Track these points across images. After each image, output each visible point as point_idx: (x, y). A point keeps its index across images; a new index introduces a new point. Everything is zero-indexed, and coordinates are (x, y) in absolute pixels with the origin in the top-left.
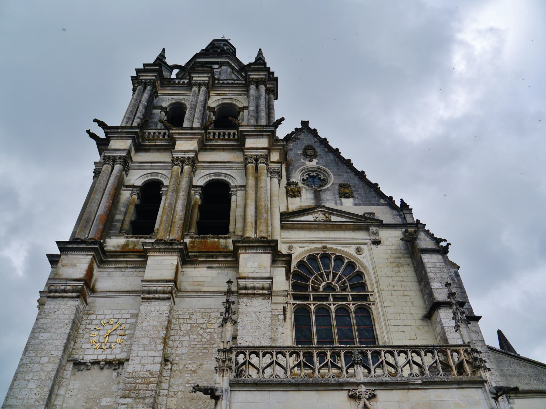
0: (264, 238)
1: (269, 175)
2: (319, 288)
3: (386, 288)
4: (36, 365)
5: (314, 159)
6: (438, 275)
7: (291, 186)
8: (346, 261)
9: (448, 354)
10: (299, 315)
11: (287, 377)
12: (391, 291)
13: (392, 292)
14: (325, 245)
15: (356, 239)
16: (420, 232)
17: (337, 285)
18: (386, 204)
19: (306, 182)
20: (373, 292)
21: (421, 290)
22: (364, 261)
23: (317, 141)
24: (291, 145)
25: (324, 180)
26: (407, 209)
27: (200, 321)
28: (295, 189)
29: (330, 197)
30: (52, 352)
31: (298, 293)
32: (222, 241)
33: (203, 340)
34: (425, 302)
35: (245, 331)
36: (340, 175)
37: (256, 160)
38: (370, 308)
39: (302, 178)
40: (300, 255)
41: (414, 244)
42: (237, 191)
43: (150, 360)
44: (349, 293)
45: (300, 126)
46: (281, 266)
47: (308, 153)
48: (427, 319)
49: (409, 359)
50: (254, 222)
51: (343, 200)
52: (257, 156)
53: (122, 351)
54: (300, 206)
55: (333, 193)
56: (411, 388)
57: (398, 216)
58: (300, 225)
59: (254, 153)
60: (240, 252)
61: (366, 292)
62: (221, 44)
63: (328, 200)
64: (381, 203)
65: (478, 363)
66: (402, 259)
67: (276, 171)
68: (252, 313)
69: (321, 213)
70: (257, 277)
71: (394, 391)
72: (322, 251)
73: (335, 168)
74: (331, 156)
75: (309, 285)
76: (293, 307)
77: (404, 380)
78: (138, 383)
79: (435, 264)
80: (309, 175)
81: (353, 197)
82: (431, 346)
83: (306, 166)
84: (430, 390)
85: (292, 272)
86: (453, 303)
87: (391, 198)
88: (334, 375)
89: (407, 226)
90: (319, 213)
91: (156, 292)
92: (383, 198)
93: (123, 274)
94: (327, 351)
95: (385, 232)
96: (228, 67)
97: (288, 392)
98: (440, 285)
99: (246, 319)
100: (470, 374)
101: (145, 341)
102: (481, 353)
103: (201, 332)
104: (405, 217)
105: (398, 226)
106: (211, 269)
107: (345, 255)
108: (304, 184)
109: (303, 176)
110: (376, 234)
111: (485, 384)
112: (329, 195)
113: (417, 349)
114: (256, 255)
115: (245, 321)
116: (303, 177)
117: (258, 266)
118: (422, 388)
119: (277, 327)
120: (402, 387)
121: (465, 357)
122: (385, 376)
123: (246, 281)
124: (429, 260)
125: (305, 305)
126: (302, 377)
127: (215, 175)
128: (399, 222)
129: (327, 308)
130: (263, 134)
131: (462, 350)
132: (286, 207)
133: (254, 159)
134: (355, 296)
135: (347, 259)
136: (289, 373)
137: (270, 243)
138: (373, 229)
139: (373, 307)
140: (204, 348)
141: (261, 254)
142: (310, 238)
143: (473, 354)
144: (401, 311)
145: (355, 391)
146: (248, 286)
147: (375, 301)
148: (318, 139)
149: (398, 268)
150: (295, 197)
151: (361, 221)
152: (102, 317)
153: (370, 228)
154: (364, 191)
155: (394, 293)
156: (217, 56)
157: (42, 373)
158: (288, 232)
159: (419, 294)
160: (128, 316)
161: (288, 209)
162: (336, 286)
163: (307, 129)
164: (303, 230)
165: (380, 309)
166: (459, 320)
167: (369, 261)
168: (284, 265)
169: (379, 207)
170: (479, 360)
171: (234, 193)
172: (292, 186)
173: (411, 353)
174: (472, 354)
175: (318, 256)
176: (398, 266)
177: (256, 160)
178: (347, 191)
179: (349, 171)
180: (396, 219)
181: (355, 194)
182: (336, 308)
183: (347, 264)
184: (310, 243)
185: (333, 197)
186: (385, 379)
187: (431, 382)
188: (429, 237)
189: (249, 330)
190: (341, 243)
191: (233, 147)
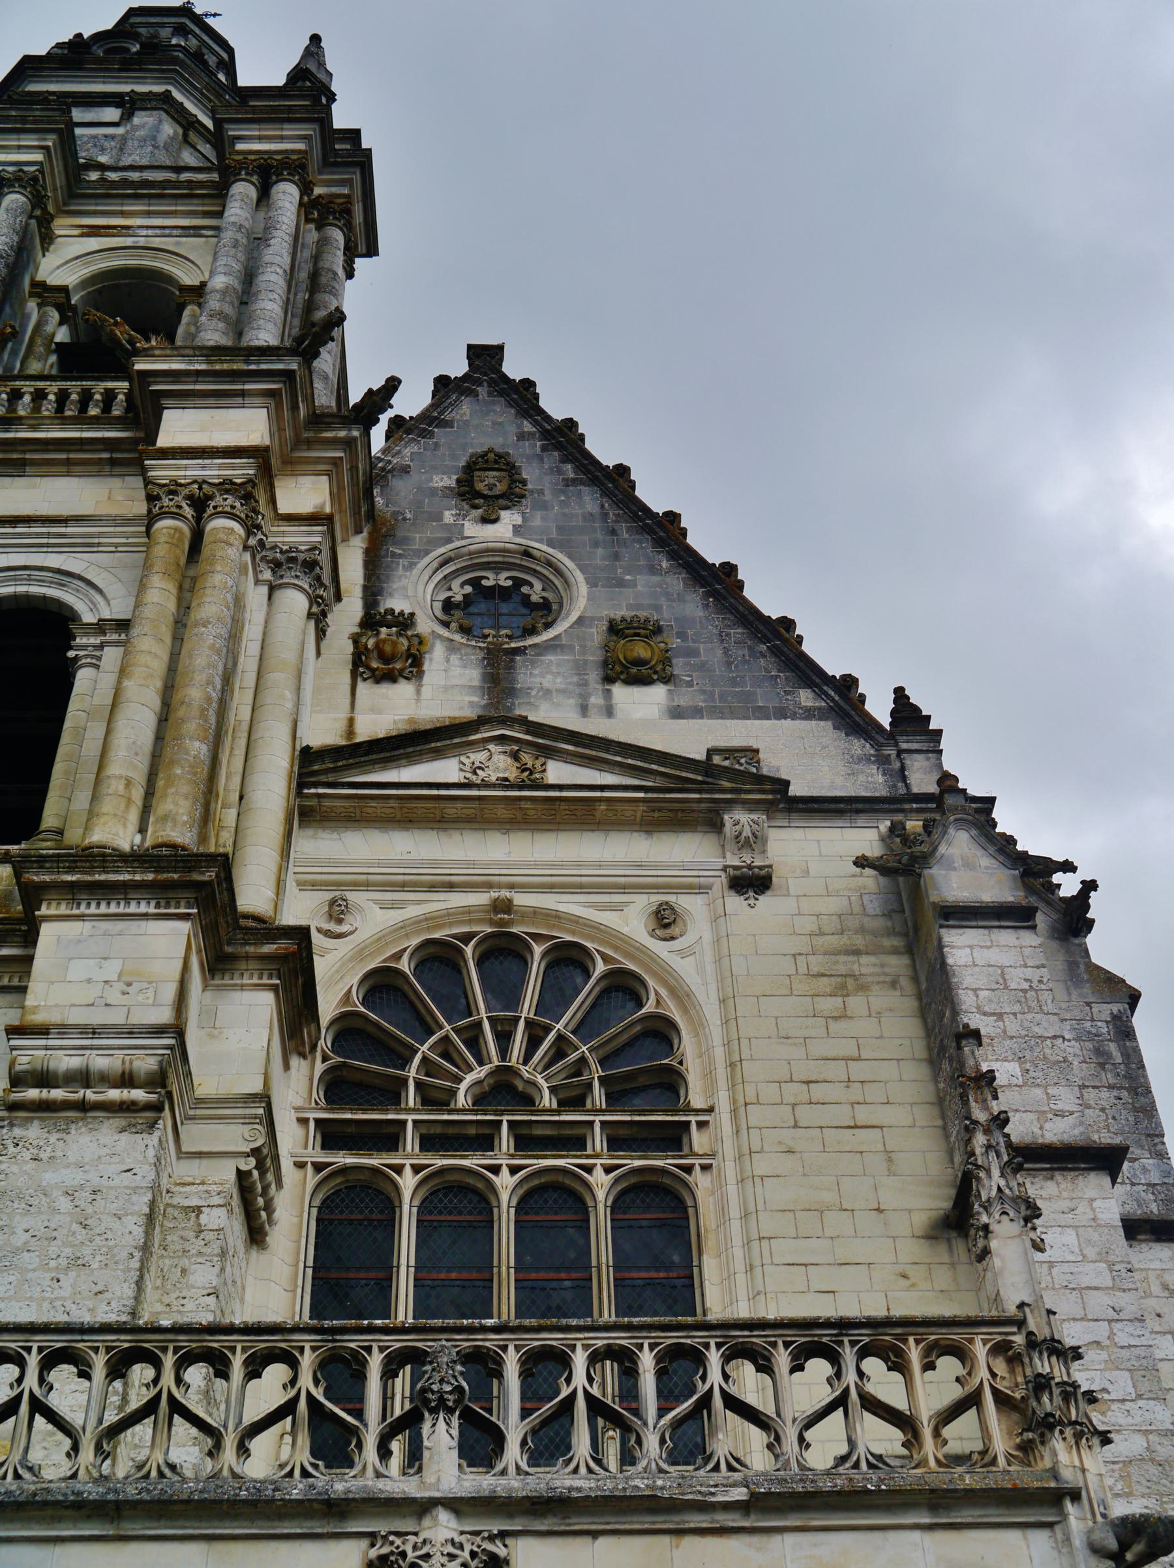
0: (174, 846)
1: (267, 575)
2: (453, 1093)
5: (505, 515)
6: (1012, 1026)
7: (378, 633)
8: (600, 967)
9: (909, 1361)
10: (341, 1221)
11: (74, 1476)
12: (794, 1106)
13: (798, 1109)
14: (505, 893)
15: (656, 867)
16: (951, 831)
17: (540, 1080)
18: (820, 708)
19: (458, 614)
20: (711, 1110)
22: (686, 969)
23: (529, 433)
24: (407, 451)
25: (545, 605)
26: (915, 733)
28: (394, 644)
29: (559, 680)
31: (348, 1116)
34: (950, 1153)
35: (12, 1278)
36: (621, 583)
37: (200, 504)
38: (686, 1185)
39: (443, 596)
40: (381, 940)
41: (918, 884)
42: (101, 646)
45: (458, 367)
46: (255, 981)
47: (480, 486)
48: (954, 1234)
49: (707, 1386)
50: (140, 776)
51: (620, 692)
52: (201, 483)
54: (411, 721)
55: (576, 661)
56: (692, 1525)
57: (873, 762)
58: (392, 803)
59: (190, 471)
60: (44, 910)
61: (676, 1112)
62: (162, 25)
63: (548, 693)
64: (798, 704)
65: (1048, 1404)
66: (864, 959)
67: (301, 556)
68: (55, 1193)
69: (500, 748)
70: (104, 1026)
71: (602, 1541)
72: (492, 923)
73: (600, 551)
74: (587, 499)
75: (404, 1081)
76: (312, 1179)
77: (662, 1488)
79: (1003, 975)
81: (667, 680)
82: (828, 1324)
83: (464, 543)
84: (790, 1539)
85: (333, 1022)
86: (976, 1122)
87: (849, 682)
88: (315, 1466)
89: (907, 806)
90: (492, 747)
92: (809, 684)
94: (301, 1350)
95: (799, 834)
96: (164, 116)
97: (59, 1550)
99: (21, 1223)
100: (1001, 1461)
102: (1078, 1356)
104: (903, 769)
105: (860, 806)
107: (602, 942)
108: (446, 625)
109: (450, 589)
110: (752, 842)
111: (1069, 1507)
112: (554, 669)
113: (757, 1339)
114: (120, 925)
115: (19, 1231)
116: (450, 594)
117: (120, 975)
118: (746, 1524)
119: (185, 1262)
120: (646, 1522)
121: (994, 1375)
122: (572, 1466)
123: (51, 1042)
125: (375, 1171)
126: (147, 1476)
127: (15, 579)
129: (480, 1185)
130: (247, 387)
131: (985, 1342)
132: (341, 726)
133: (190, 498)
134: (623, 1132)
135: (606, 959)
136: (87, 1454)
137: (191, 869)
138: (739, 819)
139: (701, 1182)
141: (143, 924)
142: (435, 864)
143: (1031, 1360)
144: (829, 1197)
145: (398, 1542)
146: (53, 1065)
147: (713, 1155)
148: (535, 423)
149: (840, 999)
150: (390, 677)
151: (684, 785)
153: (726, 817)
154: (726, 651)
156: (120, 70)
158: (335, 836)
161: (350, 731)
162: (534, 1084)
163: (492, 383)
164: (407, 829)
165: (732, 1189)
166: (988, 1201)
167: (710, 968)
168: (270, 977)
169: (787, 723)
170: (1056, 1391)
171: (86, 656)
172: (384, 630)
173: (727, 1359)
174: (1026, 1360)
176: (841, 991)
177: (200, 504)
178: (641, 650)
179: (665, 564)
180: (862, 778)
181: (679, 666)
182: (526, 1187)
183: (603, 984)
184: (433, 887)
185: (575, 679)
186: (568, 1483)
187: (793, 1495)
188: (992, 850)
189: (30, 1275)
190: (581, 886)
191: (111, 451)
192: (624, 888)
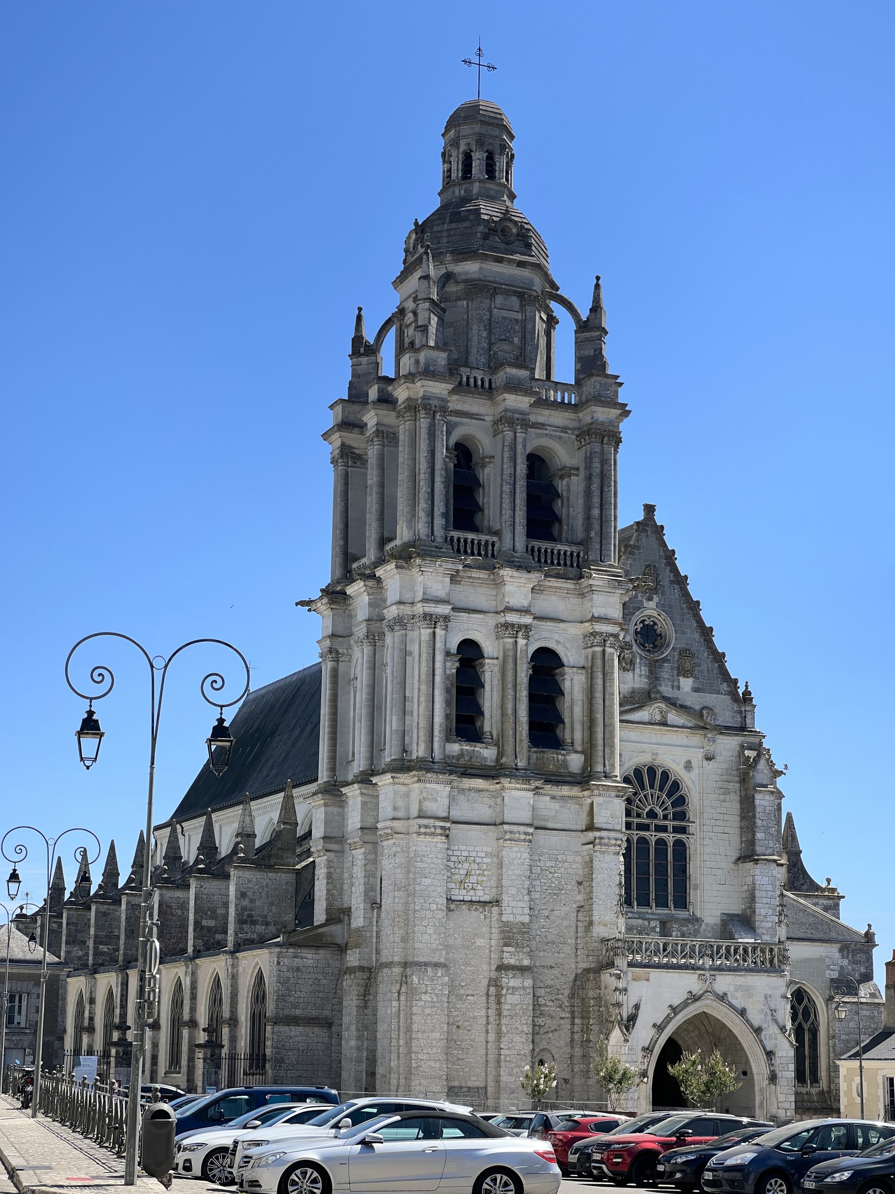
3: (708, 822)
4: (428, 912)
5: (654, 596)
21: (741, 828)
27: (549, 864)
30: (437, 899)
32: (560, 757)
33: (553, 885)
34: (742, 842)
43: (520, 911)
44: (670, 824)
51: (682, 679)
54: (633, 688)
66: (731, 784)
78: (514, 933)
80: (644, 621)
87: (736, 681)
93: (468, 800)
98: (763, 834)
101: (513, 891)
104: (745, 717)
124: (762, 801)
140: (554, 894)
144: (717, 851)
152: (458, 853)
155: (715, 829)
157: (434, 920)
159: (738, 831)
160: (483, 855)
176: (725, 794)
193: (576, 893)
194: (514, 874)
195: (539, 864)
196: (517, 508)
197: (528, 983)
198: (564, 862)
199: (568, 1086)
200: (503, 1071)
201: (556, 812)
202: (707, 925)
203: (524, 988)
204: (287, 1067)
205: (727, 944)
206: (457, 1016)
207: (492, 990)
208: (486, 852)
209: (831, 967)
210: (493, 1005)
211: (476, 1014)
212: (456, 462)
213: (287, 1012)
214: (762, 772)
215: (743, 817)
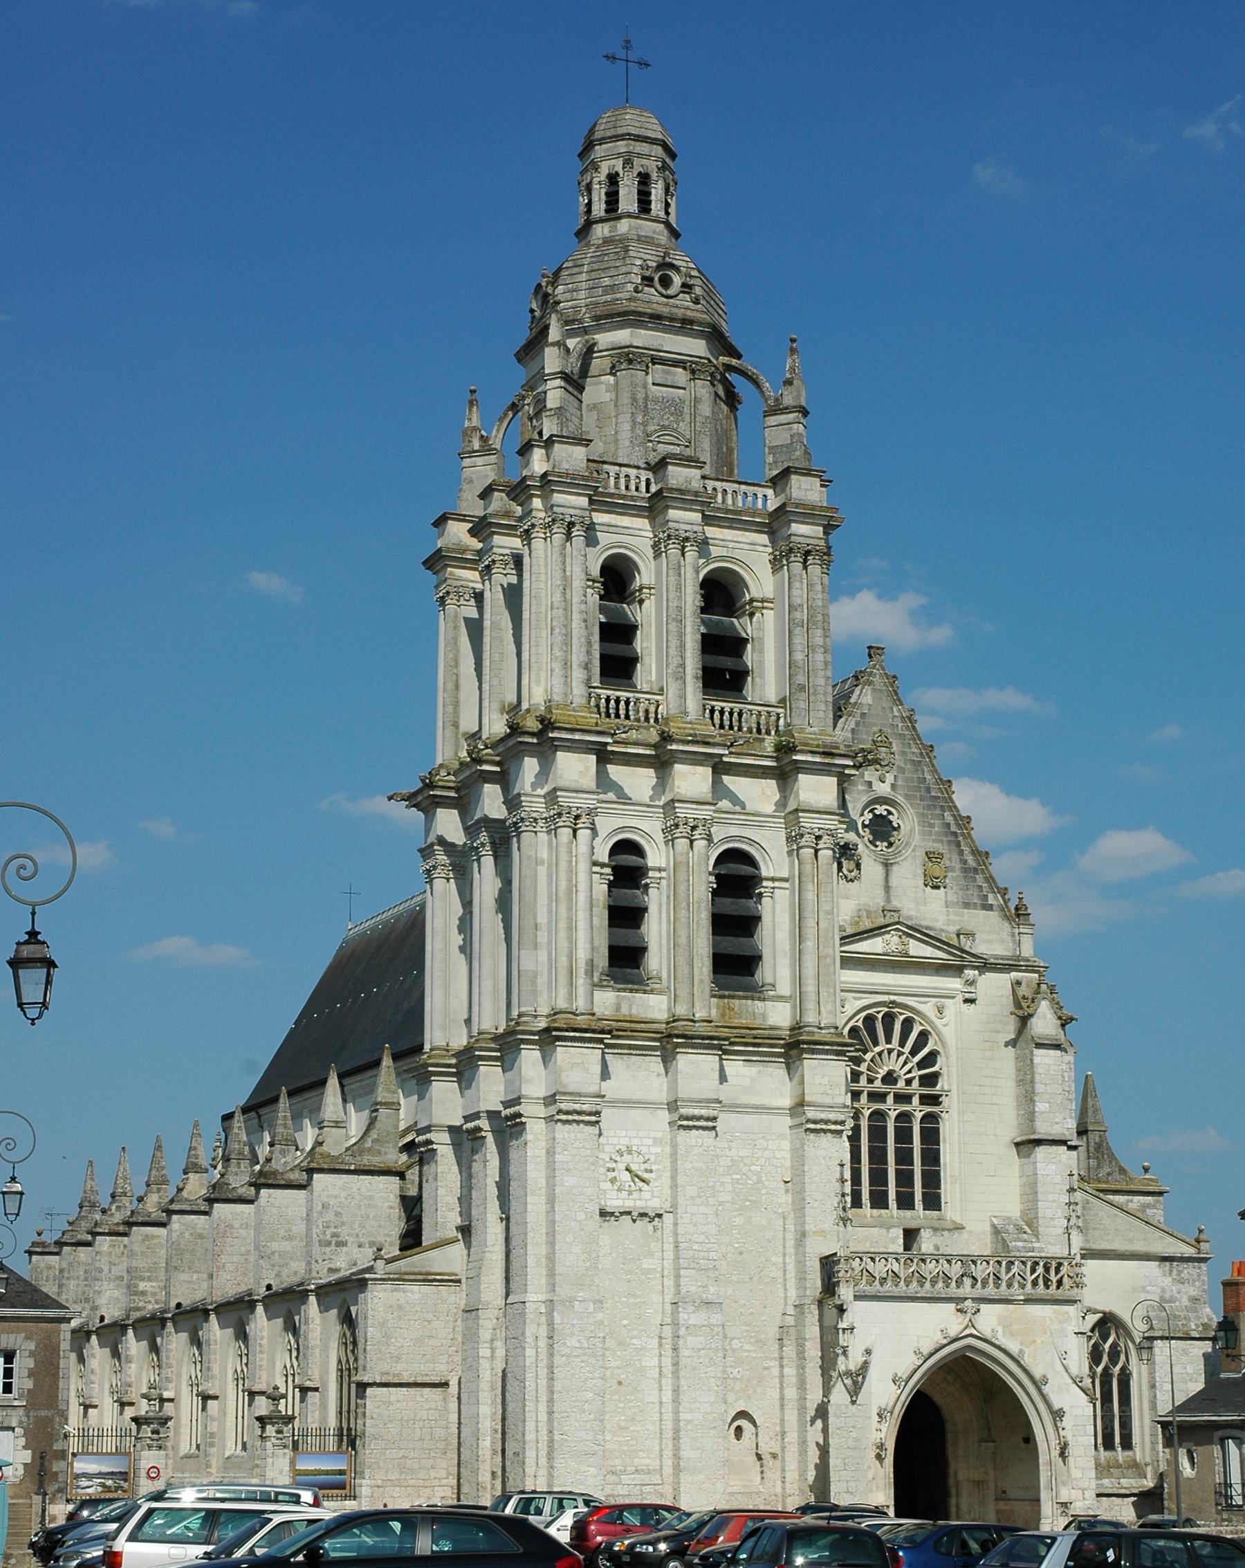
4: (573, 1223)
22: (946, 1031)
27: (743, 1153)
33: (749, 1182)
53: (653, 1196)
54: (859, 904)
91: (699, 1118)
93: (628, 1066)
98: (1047, 1105)
101: (691, 1191)
103: (745, 1170)
106: (749, 1063)
110: (971, 983)
128: (1008, 951)
130: (833, 769)
138: (970, 973)
150: (852, 881)
152: (615, 1141)
175: (880, 1016)
192: (929, 996)
193: (782, 1191)
194: (693, 1167)
195: (730, 1154)
196: (689, 654)
197: (716, 1318)
198: (766, 1149)
199: (778, 1463)
200: (685, 1442)
201: (752, 1080)
202: (971, 1232)
203: (709, 1326)
204: (386, 1444)
205: (996, 1259)
206: (618, 1368)
207: (668, 1331)
208: (654, 1138)
209: (1148, 1288)
210: (668, 1351)
211: (644, 1364)
212: (602, 592)
213: (385, 1367)
214: (1045, 1017)
215: (1020, 1082)
